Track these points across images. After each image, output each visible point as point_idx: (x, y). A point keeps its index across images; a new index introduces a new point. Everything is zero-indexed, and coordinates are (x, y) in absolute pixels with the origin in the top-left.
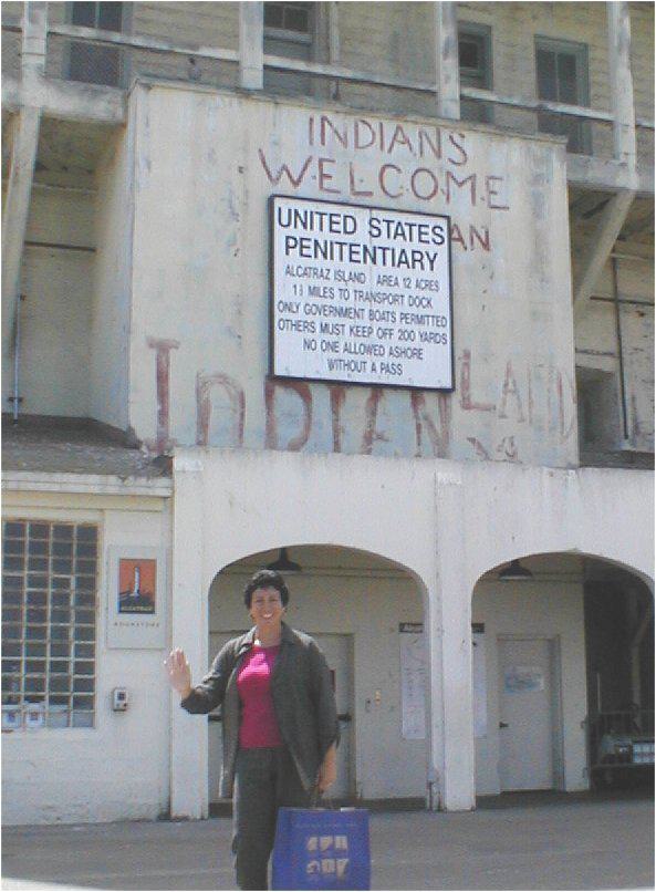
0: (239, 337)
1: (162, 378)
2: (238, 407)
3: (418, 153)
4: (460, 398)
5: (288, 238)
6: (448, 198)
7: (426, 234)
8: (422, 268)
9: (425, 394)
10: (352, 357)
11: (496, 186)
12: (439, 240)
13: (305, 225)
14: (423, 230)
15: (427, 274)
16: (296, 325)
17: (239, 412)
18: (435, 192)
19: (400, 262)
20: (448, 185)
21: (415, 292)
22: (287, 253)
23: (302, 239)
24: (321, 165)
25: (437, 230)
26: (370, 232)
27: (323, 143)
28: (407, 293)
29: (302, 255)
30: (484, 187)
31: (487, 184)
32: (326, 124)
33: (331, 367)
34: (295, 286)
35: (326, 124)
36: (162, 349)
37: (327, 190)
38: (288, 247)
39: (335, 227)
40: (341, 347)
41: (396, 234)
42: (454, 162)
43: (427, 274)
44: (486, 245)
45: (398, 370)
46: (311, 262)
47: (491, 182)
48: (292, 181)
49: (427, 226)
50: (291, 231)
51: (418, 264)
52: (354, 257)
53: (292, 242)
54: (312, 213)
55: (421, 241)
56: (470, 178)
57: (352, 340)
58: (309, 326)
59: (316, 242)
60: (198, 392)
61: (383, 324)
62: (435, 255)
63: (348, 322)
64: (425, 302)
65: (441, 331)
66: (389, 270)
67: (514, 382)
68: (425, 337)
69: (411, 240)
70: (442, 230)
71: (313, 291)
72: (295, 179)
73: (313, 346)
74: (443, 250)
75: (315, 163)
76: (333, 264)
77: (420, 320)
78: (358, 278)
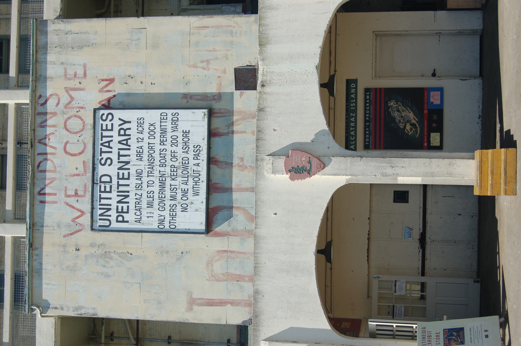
0: (182, 253)
1: (211, 303)
2: (225, 254)
3: (54, 129)
4: (214, 101)
5: (117, 221)
6: (82, 108)
7: (107, 125)
8: (130, 129)
9: (213, 127)
10: (191, 179)
11: (71, 72)
12: (110, 117)
13: (109, 209)
14: (104, 128)
15: (133, 126)
16: (173, 217)
17: (229, 254)
18: (80, 118)
19: (127, 144)
20: (73, 108)
21: (146, 135)
22: (127, 222)
23: (117, 212)
24: (69, 196)
25: (104, 117)
26: (109, 165)
27: (55, 194)
28: (146, 140)
29: (127, 212)
30: (72, 81)
31: (70, 79)
32: (41, 192)
33: (196, 194)
34: (148, 217)
35: (41, 192)
36: (192, 302)
37: (85, 192)
38: (123, 221)
39: (108, 189)
40: (184, 187)
41: (109, 147)
42: (58, 104)
43: (133, 126)
44: (112, 81)
45: (197, 147)
46: (132, 206)
47: (68, 76)
48: (81, 215)
49: (102, 124)
50: (113, 218)
51: (128, 132)
52: (126, 176)
53: (120, 219)
54: (100, 205)
55: (112, 130)
56: (67, 92)
57: (179, 179)
58: (173, 209)
59: (119, 202)
60: (218, 280)
61: (168, 157)
62: (120, 119)
63: (168, 181)
64: (152, 128)
65: (170, 117)
66: (133, 152)
67: (202, 62)
68: (175, 128)
69: (112, 137)
70: (103, 114)
71: (150, 205)
72: (80, 213)
73: (186, 206)
74: (118, 114)
75: (69, 200)
76: (132, 188)
77: (164, 132)
78: (139, 175)
